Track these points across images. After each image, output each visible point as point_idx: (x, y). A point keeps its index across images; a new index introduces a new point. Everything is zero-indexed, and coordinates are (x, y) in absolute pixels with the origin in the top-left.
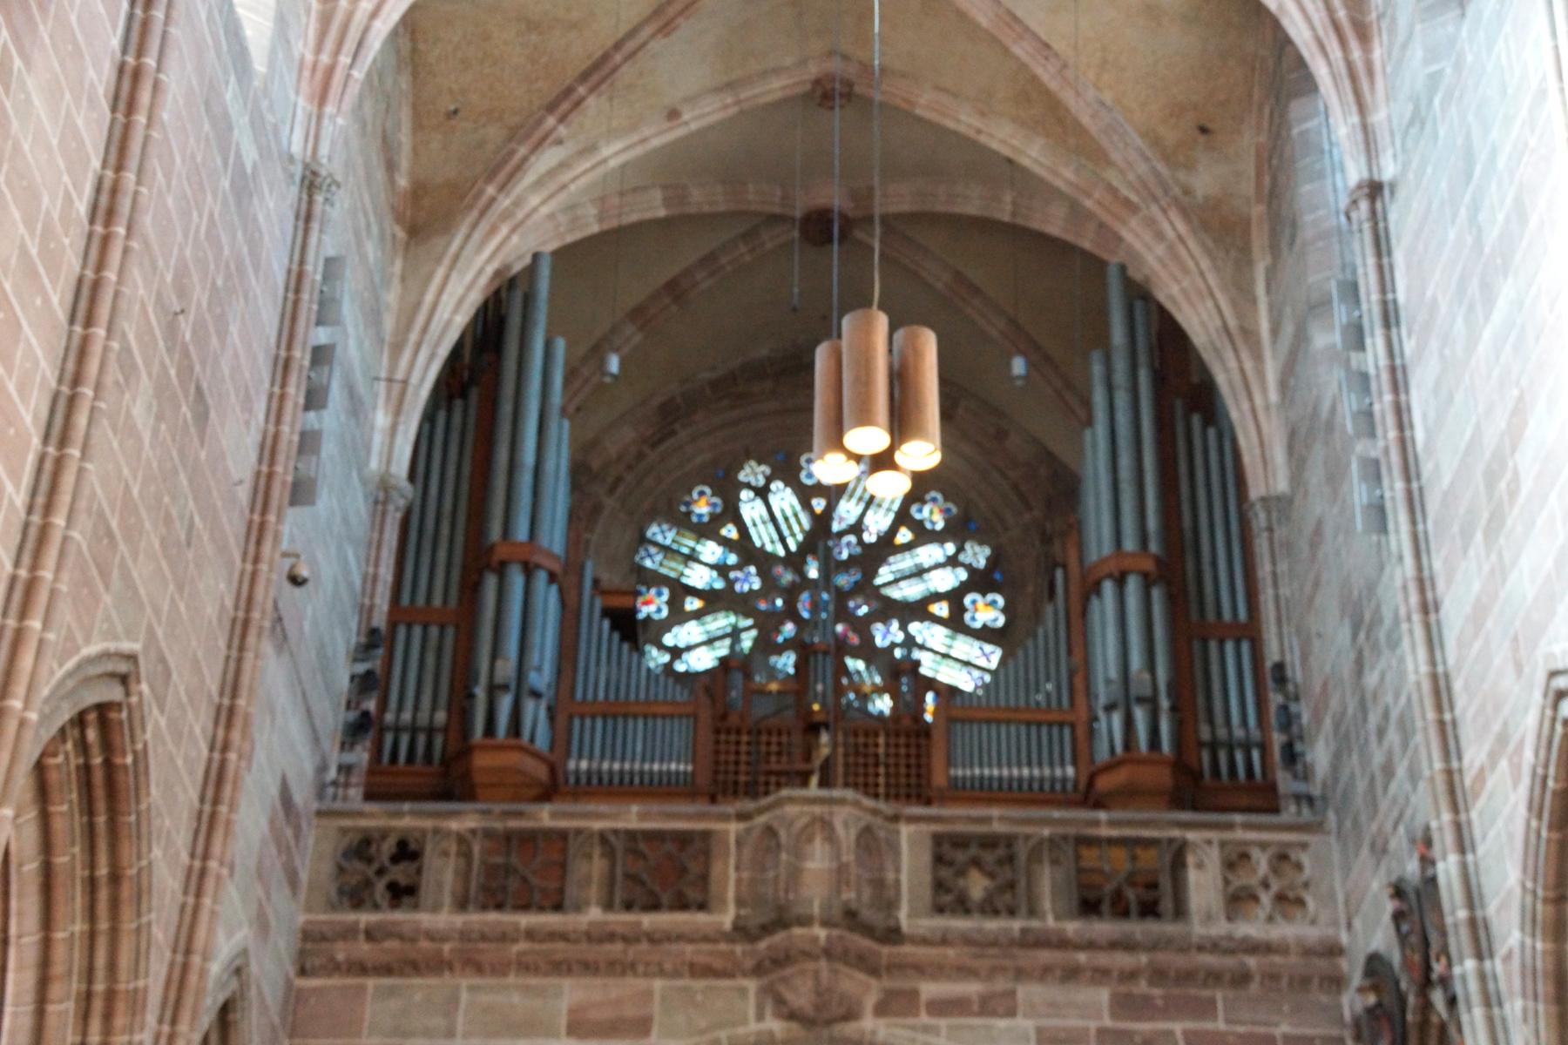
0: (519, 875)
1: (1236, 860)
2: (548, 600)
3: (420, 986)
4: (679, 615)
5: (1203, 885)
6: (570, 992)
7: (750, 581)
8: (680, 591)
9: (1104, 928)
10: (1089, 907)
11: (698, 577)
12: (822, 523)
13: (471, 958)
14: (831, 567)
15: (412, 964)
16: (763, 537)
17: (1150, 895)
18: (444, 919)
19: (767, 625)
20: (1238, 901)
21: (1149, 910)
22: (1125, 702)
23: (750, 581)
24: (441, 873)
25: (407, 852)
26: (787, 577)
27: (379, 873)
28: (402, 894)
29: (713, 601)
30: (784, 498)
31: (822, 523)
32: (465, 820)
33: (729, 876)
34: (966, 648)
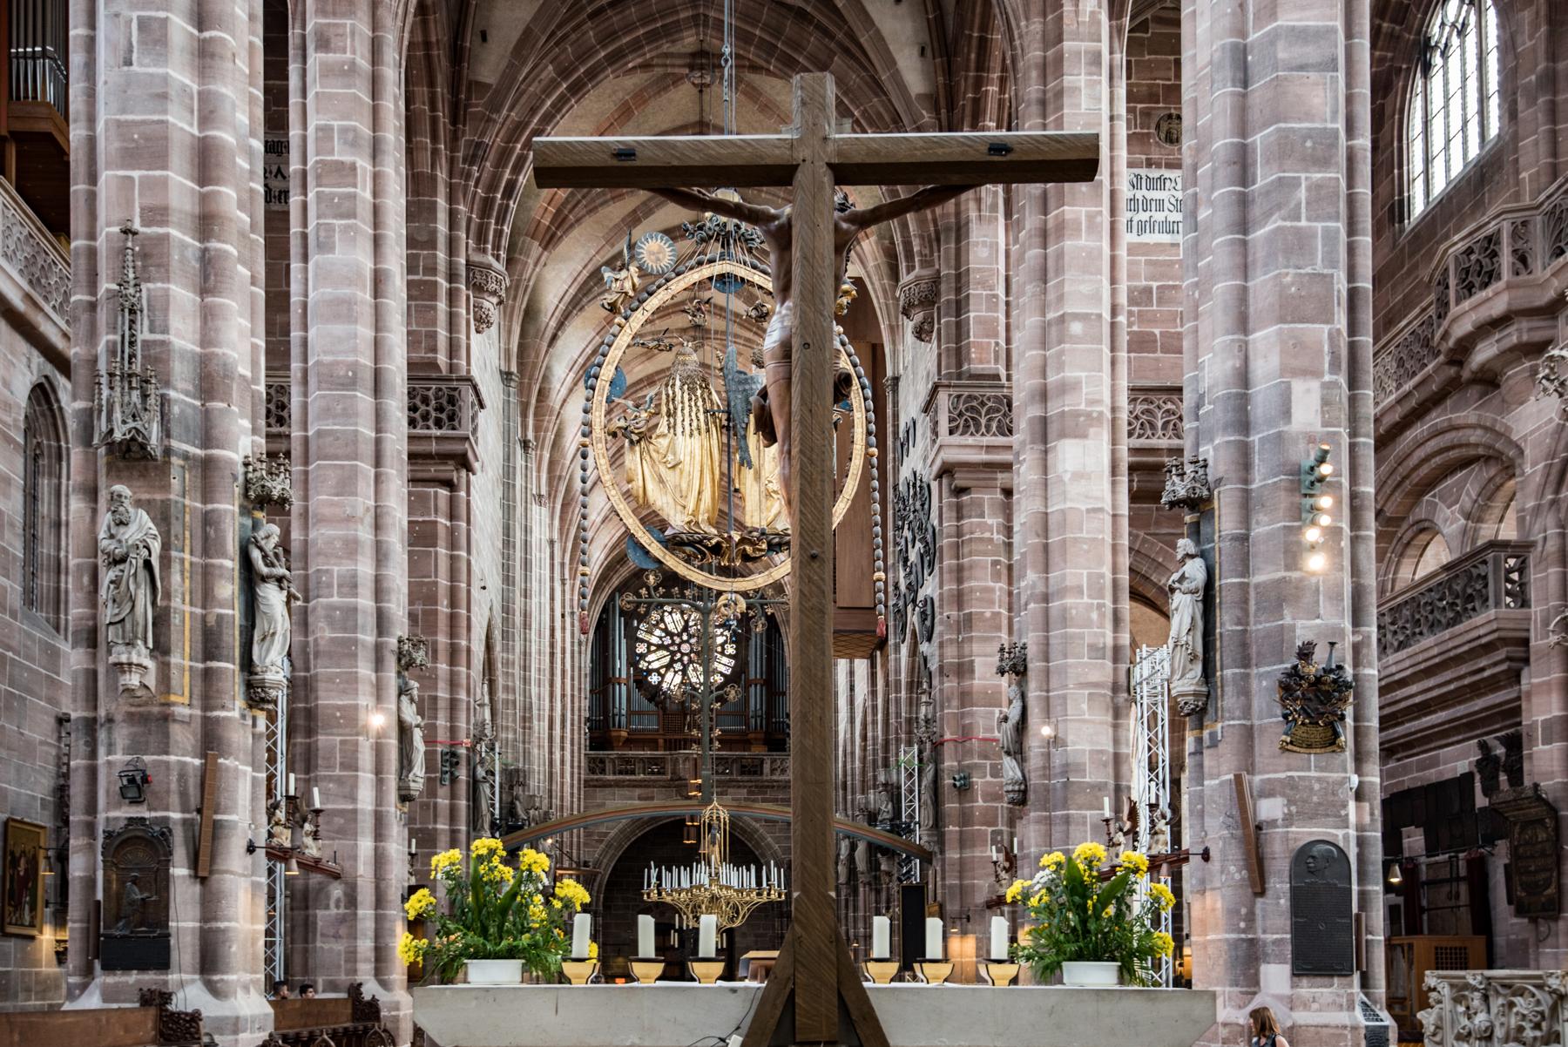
0: (627, 766)
1: (774, 761)
2: (624, 688)
3: (608, 790)
4: (649, 652)
5: (767, 767)
6: (638, 791)
7: (668, 641)
8: (650, 644)
9: (746, 778)
10: (743, 773)
11: (655, 640)
12: (686, 622)
13: (618, 784)
14: (690, 636)
15: (606, 785)
16: (671, 627)
17: (753, 768)
18: (611, 777)
19: (673, 654)
20: (773, 771)
21: (755, 773)
22: (756, 717)
23: (668, 641)
24: (609, 766)
25: (602, 761)
26: (677, 640)
27: (595, 765)
28: (603, 771)
29: (660, 647)
30: (677, 616)
31: (686, 622)
32: (614, 753)
33: (669, 767)
34: (725, 660)
